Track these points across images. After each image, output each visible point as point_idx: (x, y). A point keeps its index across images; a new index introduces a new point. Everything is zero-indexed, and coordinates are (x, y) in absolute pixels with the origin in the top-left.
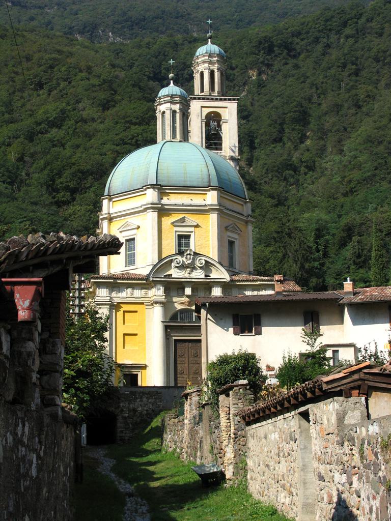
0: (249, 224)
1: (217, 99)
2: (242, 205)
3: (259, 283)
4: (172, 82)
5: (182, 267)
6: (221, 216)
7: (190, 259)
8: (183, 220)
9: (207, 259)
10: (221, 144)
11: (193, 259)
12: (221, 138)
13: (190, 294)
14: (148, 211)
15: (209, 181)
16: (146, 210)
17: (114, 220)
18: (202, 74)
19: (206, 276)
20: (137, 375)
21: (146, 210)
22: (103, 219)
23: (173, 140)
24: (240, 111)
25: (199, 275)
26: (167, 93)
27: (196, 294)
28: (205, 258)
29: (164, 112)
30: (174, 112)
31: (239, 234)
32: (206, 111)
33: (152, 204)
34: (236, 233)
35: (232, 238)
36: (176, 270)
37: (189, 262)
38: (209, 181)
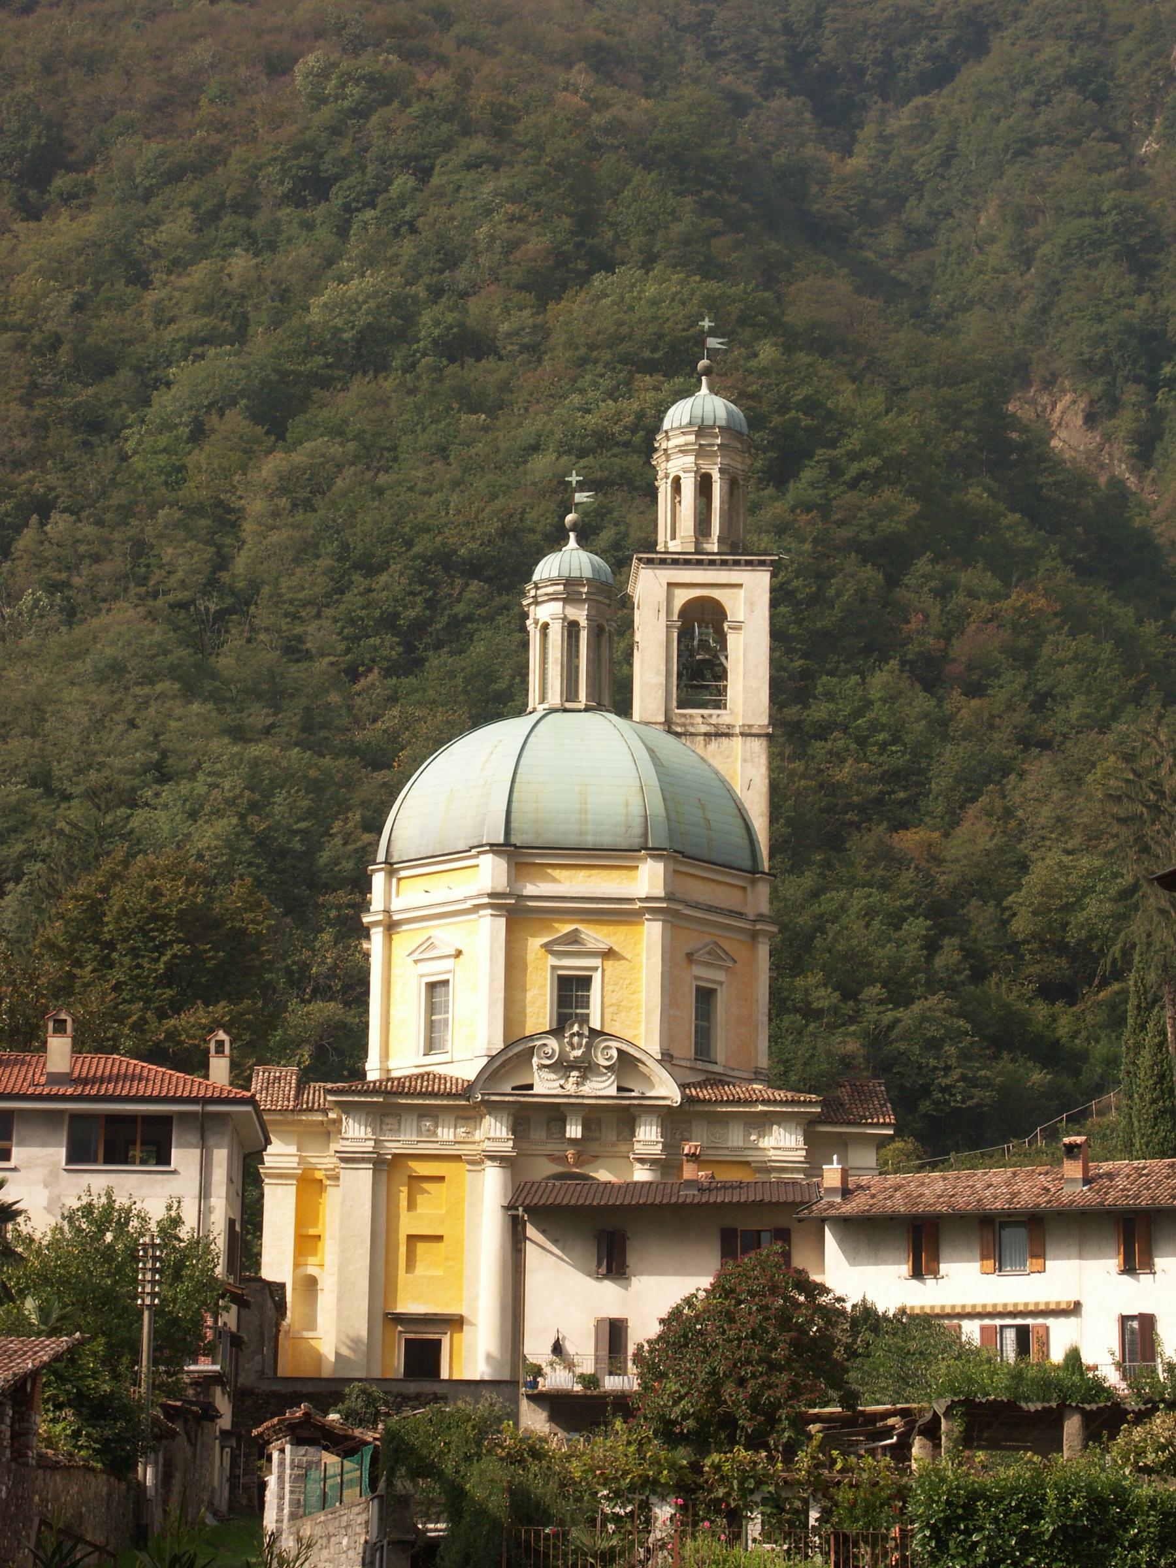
0: (760, 939)
1: (712, 563)
2: (744, 888)
3: (760, 1108)
4: (572, 535)
5: (562, 1066)
6: (673, 926)
7: (580, 1046)
8: (573, 938)
9: (624, 1047)
10: (722, 691)
11: (589, 1046)
12: (725, 671)
13: (579, 1136)
14: (482, 912)
15: (645, 835)
16: (477, 908)
17: (405, 927)
18: (677, 484)
19: (620, 1089)
20: (439, 1341)
21: (477, 908)
22: (376, 924)
23: (568, 705)
24: (779, 596)
25: (603, 1087)
26: (555, 574)
27: (597, 1134)
28: (618, 1045)
29: (546, 626)
30: (572, 628)
31: (727, 969)
32: (682, 597)
33: (492, 895)
34: (720, 967)
35: (707, 980)
36: (547, 1075)
37: (578, 1053)
38: (645, 835)
